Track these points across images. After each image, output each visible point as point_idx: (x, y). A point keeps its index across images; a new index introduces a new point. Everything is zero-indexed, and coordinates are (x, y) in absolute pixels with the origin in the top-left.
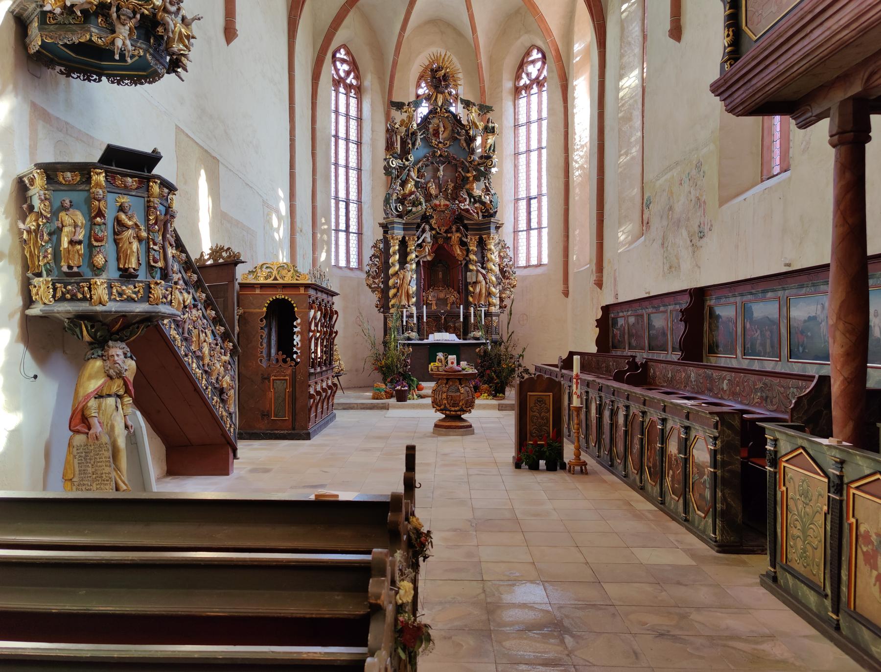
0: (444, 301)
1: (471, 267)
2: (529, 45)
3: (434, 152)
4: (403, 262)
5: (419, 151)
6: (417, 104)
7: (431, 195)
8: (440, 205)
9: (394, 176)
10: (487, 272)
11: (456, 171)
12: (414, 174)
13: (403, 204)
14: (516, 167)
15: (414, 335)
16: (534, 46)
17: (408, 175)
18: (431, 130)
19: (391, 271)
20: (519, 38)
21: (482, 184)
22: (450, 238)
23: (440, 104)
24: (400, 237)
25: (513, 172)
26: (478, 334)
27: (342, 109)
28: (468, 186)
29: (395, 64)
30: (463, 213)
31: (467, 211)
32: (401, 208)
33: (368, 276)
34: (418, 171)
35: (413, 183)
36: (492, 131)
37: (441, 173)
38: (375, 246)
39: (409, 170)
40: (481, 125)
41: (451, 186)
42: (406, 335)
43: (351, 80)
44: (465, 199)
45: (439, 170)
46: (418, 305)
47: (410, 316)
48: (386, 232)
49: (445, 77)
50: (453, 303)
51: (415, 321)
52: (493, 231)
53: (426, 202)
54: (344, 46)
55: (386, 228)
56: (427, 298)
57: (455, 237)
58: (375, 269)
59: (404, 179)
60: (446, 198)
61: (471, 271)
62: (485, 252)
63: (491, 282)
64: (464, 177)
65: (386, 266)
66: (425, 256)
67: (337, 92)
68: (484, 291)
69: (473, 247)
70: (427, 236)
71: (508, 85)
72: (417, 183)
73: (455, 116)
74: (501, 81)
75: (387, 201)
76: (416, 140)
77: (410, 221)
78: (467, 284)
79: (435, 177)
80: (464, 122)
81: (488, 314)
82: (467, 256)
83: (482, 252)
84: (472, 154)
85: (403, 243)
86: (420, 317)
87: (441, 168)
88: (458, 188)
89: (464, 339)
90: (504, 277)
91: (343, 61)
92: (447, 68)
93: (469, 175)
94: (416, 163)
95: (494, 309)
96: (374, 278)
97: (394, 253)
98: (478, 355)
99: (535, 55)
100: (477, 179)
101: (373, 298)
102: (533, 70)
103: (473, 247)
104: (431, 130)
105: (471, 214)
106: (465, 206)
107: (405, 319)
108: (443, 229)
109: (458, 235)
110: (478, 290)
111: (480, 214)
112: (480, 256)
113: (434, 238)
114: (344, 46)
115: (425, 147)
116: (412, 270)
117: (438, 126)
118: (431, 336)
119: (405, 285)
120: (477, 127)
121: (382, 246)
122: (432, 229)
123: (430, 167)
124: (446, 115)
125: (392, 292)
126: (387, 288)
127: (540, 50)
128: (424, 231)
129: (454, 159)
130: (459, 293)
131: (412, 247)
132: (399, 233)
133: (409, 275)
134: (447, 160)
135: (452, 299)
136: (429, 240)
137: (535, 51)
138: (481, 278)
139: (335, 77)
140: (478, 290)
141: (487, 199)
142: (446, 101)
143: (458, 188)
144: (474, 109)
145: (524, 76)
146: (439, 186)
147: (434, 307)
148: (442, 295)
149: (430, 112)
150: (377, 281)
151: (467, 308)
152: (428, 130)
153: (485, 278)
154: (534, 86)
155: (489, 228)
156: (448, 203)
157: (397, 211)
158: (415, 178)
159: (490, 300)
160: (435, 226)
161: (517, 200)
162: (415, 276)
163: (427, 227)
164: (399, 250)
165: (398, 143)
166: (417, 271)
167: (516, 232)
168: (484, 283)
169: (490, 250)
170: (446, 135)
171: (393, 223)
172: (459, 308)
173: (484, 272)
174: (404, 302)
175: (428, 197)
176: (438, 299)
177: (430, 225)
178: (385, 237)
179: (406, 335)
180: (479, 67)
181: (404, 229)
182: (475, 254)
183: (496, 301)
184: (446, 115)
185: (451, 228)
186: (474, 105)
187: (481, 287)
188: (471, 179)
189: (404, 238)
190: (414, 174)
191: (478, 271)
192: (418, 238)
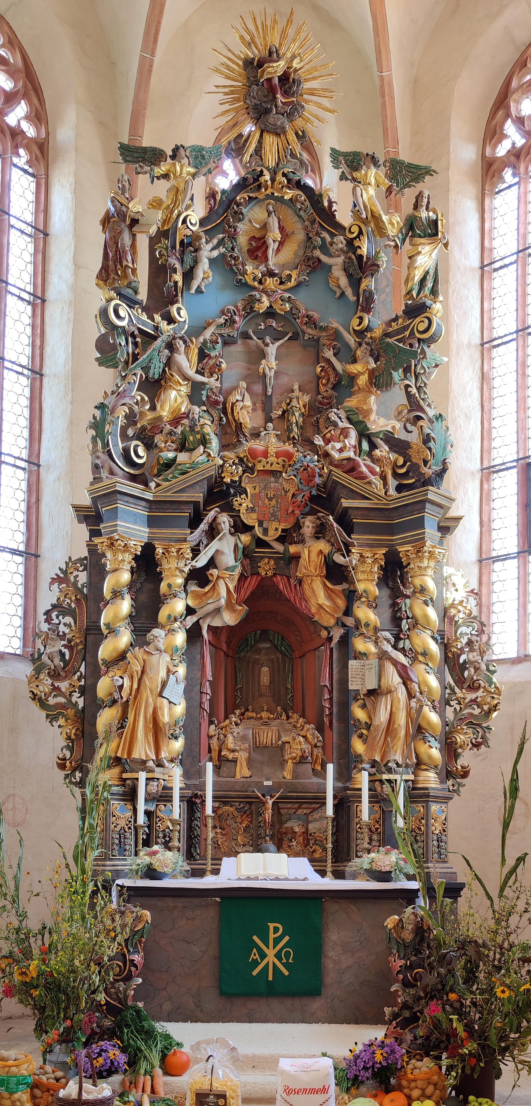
0: (276, 753)
3: (250, 303)
4: (145, 618)
5: (205, 301)
6: (202, 159)
7: (239, 426)
8: (265, 454)
9: (121, 356)
10: (414, 660)
11: (318, 358)
12: (186, 362)
13: (150, 445)
14: (485, 378)
15: (168, 859)
17: (169, 362)
18: (243, 240)
19: (105, 651)
21: (396, 396)
22: (297, 558)
23: (271, 160)
24: (136, 546)
25: (477, 394)
26: (387, 859)
28: (352, 402)
29: (145, 70)
30: (340, 476)
31: (351, 468)
32: (141, 454)
33: (38, 671)
34: (202, 355)
35: (185, 389)
36: (432, 230)
37: (270, 364)
38: (62, 579)
39: (170, 346)
40: (393, 223)
41: (301, 401)
42: (144, 859)
44: (344, 433)
45: (263, 355)
46: (190, 762)
47: (164, 797)
48: (95, 533)
49: (287, 81)
50: (302, 760)
51: (176, 815)
52: (431, 531)
53: (224, 447)
55: (91, 519)
56: (222, 744)
57: (312, 552)
58: (59, 645)
59: (155, 372)
60: (286, 437)
62: (405, 604)
63: (425, 691)
65: (93, 634)
66: (217, 611)
68: (401, 719)
69: (367, 582)
70: (226, 548)
71: (464, 153)
72: (196, 388)
73: (314, 198)
74: (445, 140)
75: (98, 426)
76: (196, 262)
77: (169, 496)
78: (346, 697)
79: (255, 378)
80: (344, 216)
81: (417, 795)
82: (348, 612)
83: (395, 606)
84: (367, 309)
86: (193, 803)
87: (272, 350)
88: (317, 412)
89: (339, 875)
90: (460, 681)
92: (293, 57)
94: (196, 331)
95: (430, 779)
96: (55, 675)
97: (117, 594)
98: (393, 940)
100: (379, 381)
101: (52, 739)
103: (367, 582)
104: (243, 240)
105: (362, 477)
106: (345, 447)
107: (141, 806)
109: (323, 546)
110: (382, 716)
111: (392, 483)
112: (387, 613)
113: (247, 556)
115: (223, 288)
116: (172, 651)
117: (265, 227)
118: (227, 863)
119: (148, 697)
120: (380, 229)
121: (83, 578)
122: (239, 527)
123: (238, 348)
124: (289, 194)
126: (94, 705)
128: (213, 532)
129: (311, 321)
130: (320, 729)
132: (132, 529)
133: (160, 664)
134: (292, 328)
135: (299, 746)
136: (229, 559)
138: (393, 678)
140: (382, 716)
141: (414, 438)
142: (287, 153)
143: (317, 412)
144: (372, 174)
145: (510, 127)
146: (265, 403)
147: (242, 771)
148: (268, 735)
149: (242, 185)
150: (64, 685)
152: (233, 237)
153: (406, 680)
155: (420, 523)
156: (289, 447)
158: (191, 373)
159: (422, 748)
160: (250, 519)
161: (488, 472)
162: (182, 670)
163: (225, 521)
164: (131, 586)
165: (144, 265)
167: (485, 560)
168: (402, 693)
169: (423, 590)
171: (112, 495)
172: (322, 774)
174: (143, 749)
175: (231, 432)
176: (257, 747)
177: (236, 516)
178: (92, 549)
179: (144, 859)
180: (384, 90)
181: (152, 522)
182: (373, 605)
184: (289, 194)
185: (298, 526)
187: (393, 709)
188: (363, 380)
189: (149, 549)
190: (186, 362)
191: (383, 656)
192: (196, 552)
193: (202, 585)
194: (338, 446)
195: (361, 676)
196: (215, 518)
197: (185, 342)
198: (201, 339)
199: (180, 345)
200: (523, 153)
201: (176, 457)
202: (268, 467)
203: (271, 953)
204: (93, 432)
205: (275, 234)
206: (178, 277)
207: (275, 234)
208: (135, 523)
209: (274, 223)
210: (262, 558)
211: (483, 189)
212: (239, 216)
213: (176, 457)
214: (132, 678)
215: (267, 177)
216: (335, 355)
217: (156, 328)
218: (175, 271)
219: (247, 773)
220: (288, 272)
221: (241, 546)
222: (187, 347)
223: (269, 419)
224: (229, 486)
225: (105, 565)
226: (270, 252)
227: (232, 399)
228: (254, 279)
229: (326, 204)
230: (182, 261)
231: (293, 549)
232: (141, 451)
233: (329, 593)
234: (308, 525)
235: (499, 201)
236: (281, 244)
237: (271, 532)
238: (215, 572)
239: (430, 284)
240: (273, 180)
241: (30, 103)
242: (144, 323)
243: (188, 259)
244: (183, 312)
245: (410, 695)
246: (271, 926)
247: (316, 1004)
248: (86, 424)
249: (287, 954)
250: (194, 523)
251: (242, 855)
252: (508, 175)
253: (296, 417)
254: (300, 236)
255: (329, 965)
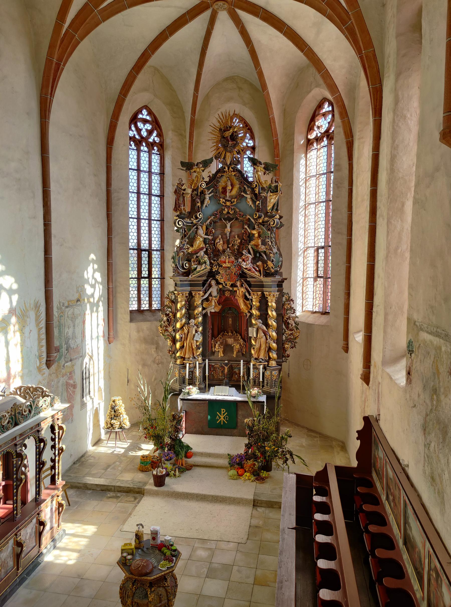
1: (254, 322)
2: (320, 98)
3: (221, 212)
7: (219, 250)
12: (201, 232)
16: (325, 100)
17: (196, 232)
20: (310, 91)
22: (236, 291)
26: (255, 391)
27: (144, 166)
28: (253, 243)
34: (207, 228)
39: (197, 228)
43: (154, 137)
45: (226, 227)
54: (146, 107)
57: (241, 291)
61: (252, 325)
64: (249, 234)
67: (139, 151)
70: (214, 290)
76: (205, 198)
85: (190, 298)
87: (228, 225)
91: (145, 121)
93: (254, 232)
99: (327, 108)
102: (322, 123)
104: (220, 188)
108: (229, 283)
109: (243, 290)
113: (221, 292)
114: (146, 107)
122: (218, 283)
125: (178, 345)
127: (331, 104)
128: (210, 286)
131: (198, 301)
136: (215, 293)
137: (326, 105)
138: (261, 334)
139: (137, 137)
140: (257, 346)
146: (228, 242)
151: (247, 363)
153: (265, 333)
154: (325, 139)
157: (183, 268)
160: (222, 281)
163: (213, 282)
166: (204, 323)
170: (234, 192)
173: (265, 328)
183: (274, 355)
186: (260, 163)
189: (190, 294)
190: (201, 232)
192: (205, 293)
193: (207, 301)
194: (245, 264)
195: (252, 332)
196: (210, 282)
197: (201, 226)
198: (207, 223)
199: (200, 227)
200: (319, 140)
201: (197, 267)
202: (226, 266)
203: (222, 417)
204: (173, 260)
205: (229, 187)
206: (199, 204)
207: (229, 187)
208: (186, 287)
209: (229, 183)
210: (226, 290)
211: (307, 149)
212: (218, 182)
213: (197, 267)
214: (185, 334)
215: (227, 168)
216: (248, 227)
217: (192, 223)
218: (198, 202)
219: (222, 355)
220: (233, 200)
221: (219, 289)
222: (202, 228)
223: (228, 247)
224: (214, 272)
225: (178, 299)
226: (228, 194)
227: (217, 241)
228: (223, 202)
229: (245, 176)
230: (200, 199)
231: (235, 289)
232: (187, 265)
233: (246, 304)
234: (238, 284)
235: (312, 153)
236: (232, 190)
237: (228, 285)
238: (210, 298)
239: (275, 208)
240: (229, 169)
241: (157, 131)
242: (188, 223)
243: (202, 198)
244: (201, 215)
245: (267, 339)
246: (222, 410)
247: (235, 431)
248: (171, 257)
249: (227, 418)
250: (203, 285)
251: (216, 387)
252: (315, 144)
253: (236, 247)
254: (238, 186)
255: (239, 421)
